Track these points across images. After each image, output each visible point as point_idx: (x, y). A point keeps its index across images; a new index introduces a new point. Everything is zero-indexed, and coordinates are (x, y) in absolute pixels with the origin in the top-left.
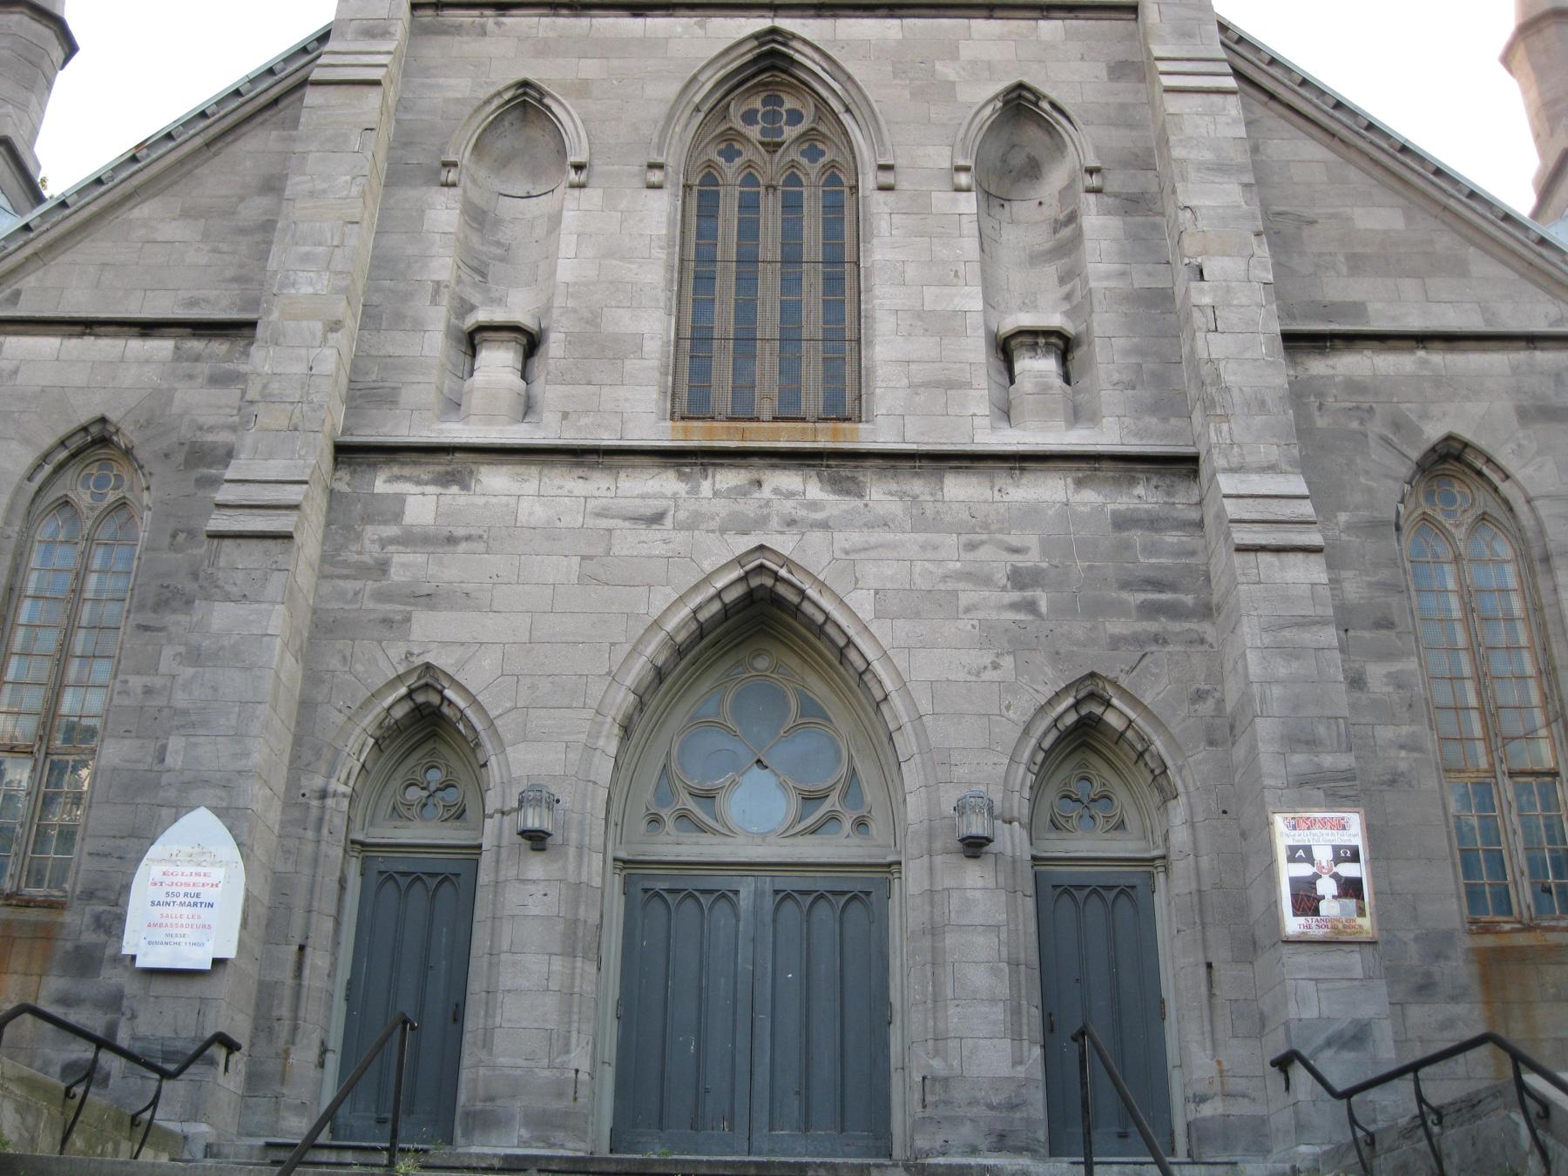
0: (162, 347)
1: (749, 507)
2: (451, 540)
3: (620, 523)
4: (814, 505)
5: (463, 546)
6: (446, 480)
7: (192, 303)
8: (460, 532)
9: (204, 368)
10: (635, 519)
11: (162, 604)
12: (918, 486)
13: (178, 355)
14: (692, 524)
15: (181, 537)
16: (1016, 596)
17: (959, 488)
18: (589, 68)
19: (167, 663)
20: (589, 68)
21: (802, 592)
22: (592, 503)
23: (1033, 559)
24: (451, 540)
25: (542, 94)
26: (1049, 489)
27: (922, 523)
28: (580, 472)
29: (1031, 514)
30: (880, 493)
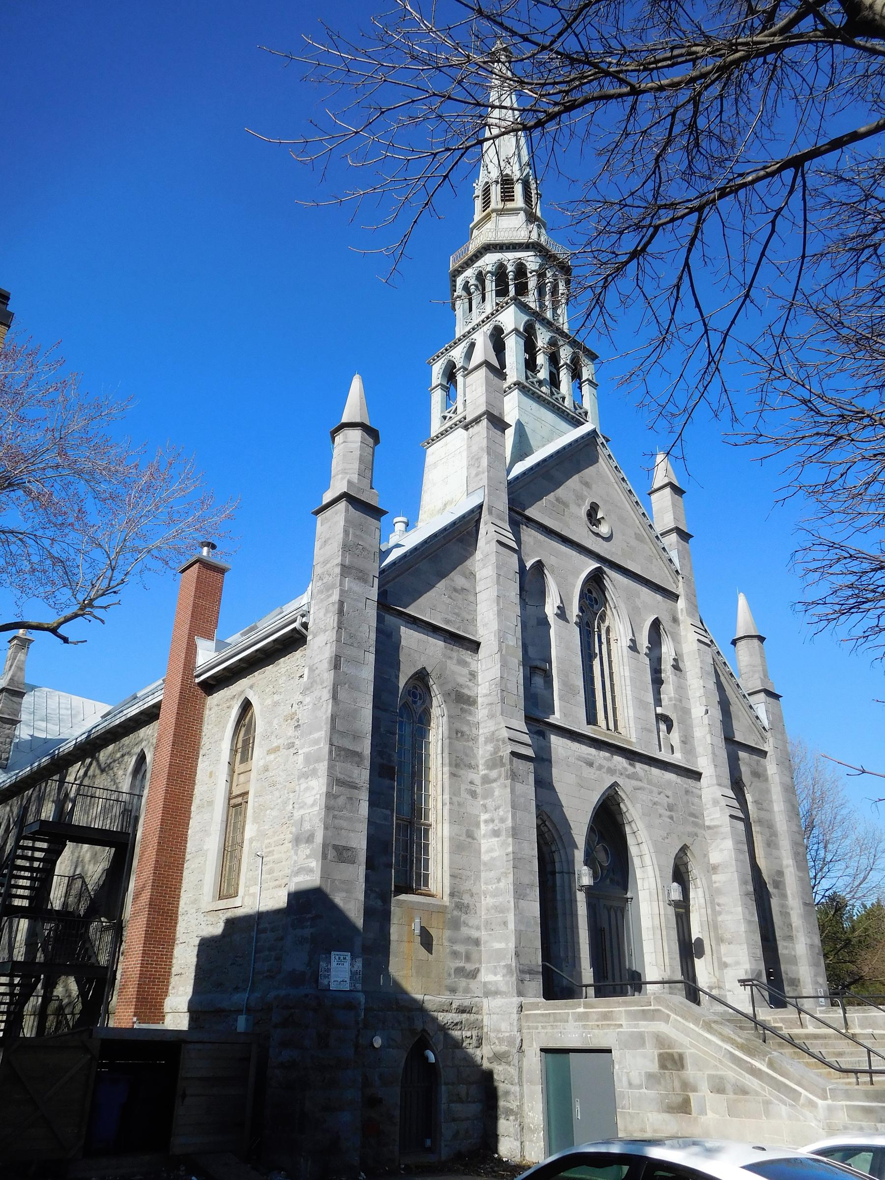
4: (626, 769)
7: (447, 622)
12: (646, 767)
14: (600, 768)
15: (459, 735)
17: (655, 771)
23: (670, 800)
25: (543, 566)
29: (669, 782)
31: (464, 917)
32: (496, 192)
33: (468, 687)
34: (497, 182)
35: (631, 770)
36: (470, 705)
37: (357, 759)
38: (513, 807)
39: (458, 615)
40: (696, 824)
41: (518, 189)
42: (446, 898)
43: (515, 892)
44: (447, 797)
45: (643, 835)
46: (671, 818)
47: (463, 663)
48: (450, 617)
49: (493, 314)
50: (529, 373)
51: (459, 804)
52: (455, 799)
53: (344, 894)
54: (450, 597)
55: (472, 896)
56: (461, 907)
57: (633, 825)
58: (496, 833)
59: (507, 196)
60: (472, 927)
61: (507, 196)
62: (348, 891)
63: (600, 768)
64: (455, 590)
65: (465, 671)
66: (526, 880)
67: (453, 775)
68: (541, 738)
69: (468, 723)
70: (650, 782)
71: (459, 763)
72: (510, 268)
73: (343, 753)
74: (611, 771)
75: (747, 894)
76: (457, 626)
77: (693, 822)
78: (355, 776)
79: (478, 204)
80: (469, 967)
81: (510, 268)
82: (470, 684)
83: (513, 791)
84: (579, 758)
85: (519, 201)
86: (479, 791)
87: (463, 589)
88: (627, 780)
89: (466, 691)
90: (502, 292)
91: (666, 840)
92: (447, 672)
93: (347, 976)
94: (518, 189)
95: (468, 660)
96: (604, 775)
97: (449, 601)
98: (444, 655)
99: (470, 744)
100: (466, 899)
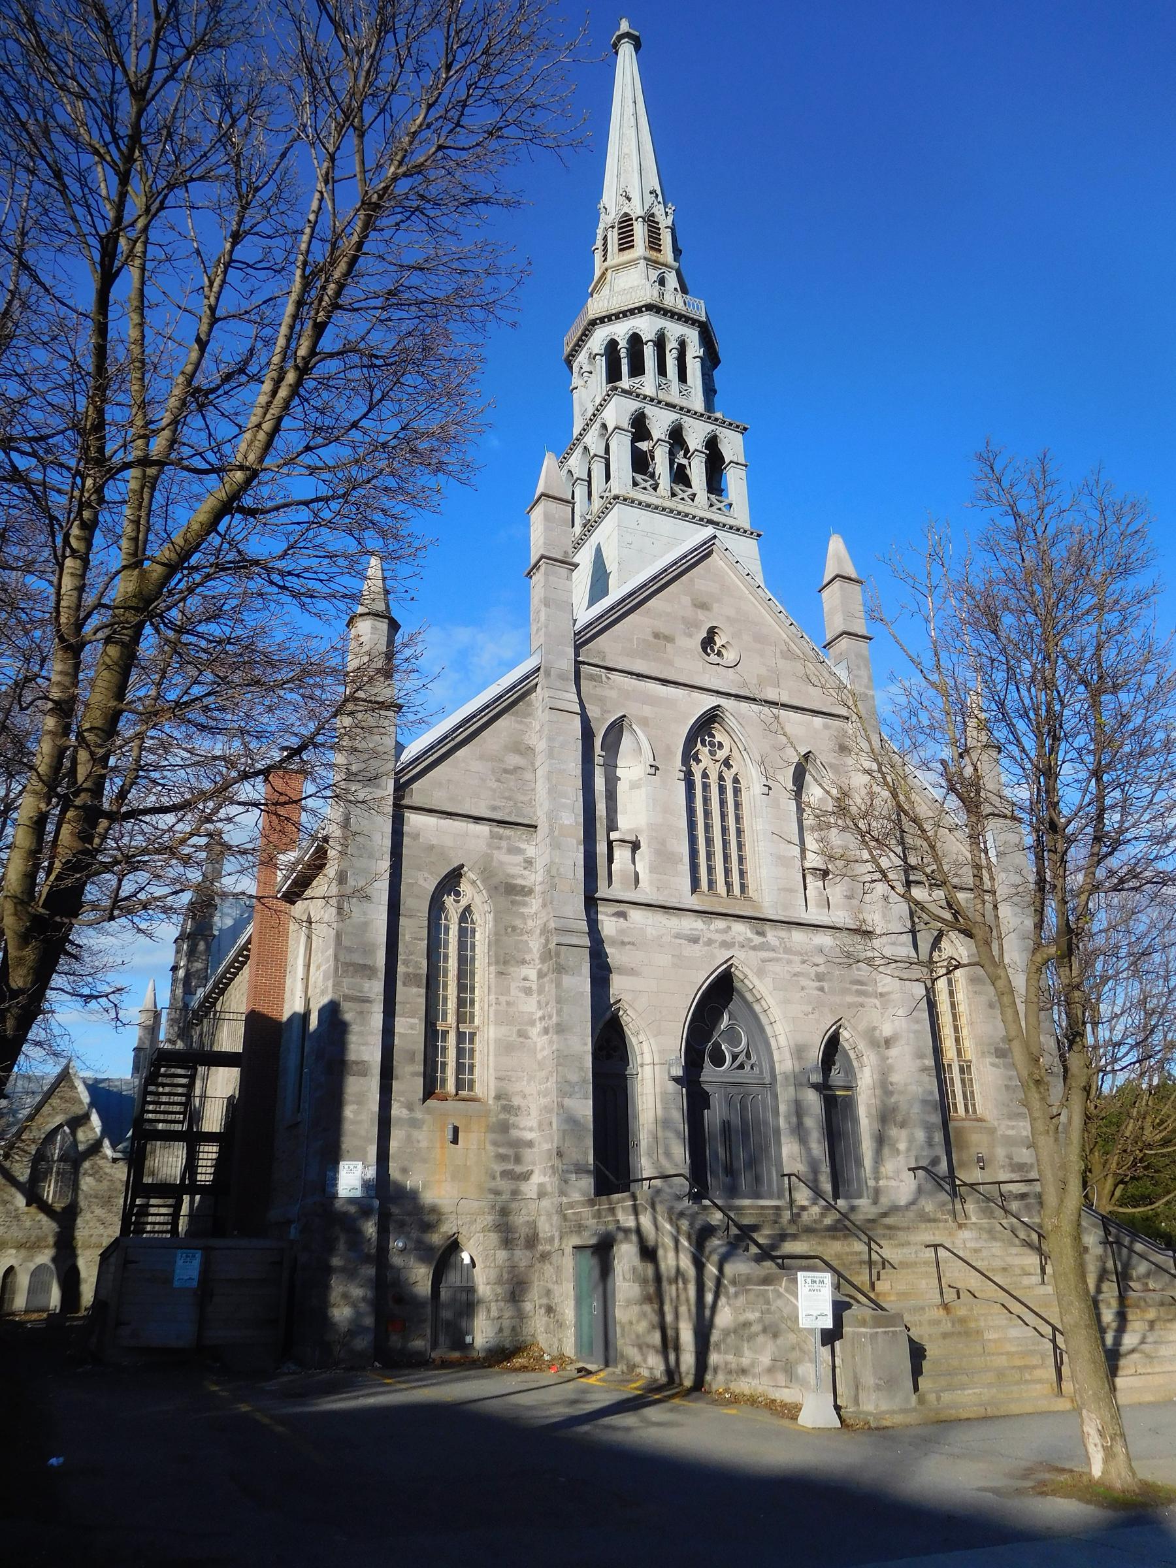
0: (483, 829)
1: (727, 937)
2: (623, 943)
3: (682, 941)
4: (750, 940)
5: (628, 947)
6: (622, 915)
7: (494, 809)
8: (626, 940)
9: (504, 844)
10: (689, 941)
11: (505, 963)
13: (493, 836)
16: (818, 984)
18: (647, 711)
19: (514, 992)
20: (647, 711)
21: (746, 976)
22: (673, 931)
24: (623, 943)
26: (824, 940)
27: (787, 951)
28: (667, 916)
30: (773, 936)
31: (512, 1119)
32: (613, 237)
33: (522, 876)
34: (613, 227)
35: (758, 940)
36: (525, 895)
37: (368, 972)
39: (509, 799)
40: (860, 993)
41: (640, 231)
42: (491, 1102)
44: (492, 997)
45: (776, 1012)
46: (821, 989)
48: (497, 803)
49: (594, 415)
50: (639, 477)
51: (508, 1003)
52: (503, 999)
53: (355, 1107)
54: (498, 781)
55: (524, 1097)
56: (509, 1109)
57: (763, 1002)
58: (546, 1031)
59: (626, 243)
60: (524, 1129)
61: (626, 243)
62: (359, 1103)
63: (710, 942)
64: (506, 771)
65: (519, 859)
66: (574, 1077)
67: (500, 973)
68: (622, 919)
69: (523, 916)
70: (787, 951)
72: (623, 344)
73: (351, 968)
74: (726, 945)
75: (924, 1069)
76: (507, 811)
77: (857, 991)
78: (366, 989)
79: (598, 256)
80: (519, 1169)
81: (623, 344)
82: (526, 873)
83: (558, 985)
84: (678, 936)
86: (534, 987)
87: (517, 769)
88: (752, 953)
89: (519, 882)
90: (613, 374)
91: (810, 1016)
92: (494, 864)
93: (358, 1184)
94: (640, 231)
95: (523, 846)
96: (716, 951)
97: (495, 785)
98: (489, 845)
99: (525, 937)
100: (516, 1101)
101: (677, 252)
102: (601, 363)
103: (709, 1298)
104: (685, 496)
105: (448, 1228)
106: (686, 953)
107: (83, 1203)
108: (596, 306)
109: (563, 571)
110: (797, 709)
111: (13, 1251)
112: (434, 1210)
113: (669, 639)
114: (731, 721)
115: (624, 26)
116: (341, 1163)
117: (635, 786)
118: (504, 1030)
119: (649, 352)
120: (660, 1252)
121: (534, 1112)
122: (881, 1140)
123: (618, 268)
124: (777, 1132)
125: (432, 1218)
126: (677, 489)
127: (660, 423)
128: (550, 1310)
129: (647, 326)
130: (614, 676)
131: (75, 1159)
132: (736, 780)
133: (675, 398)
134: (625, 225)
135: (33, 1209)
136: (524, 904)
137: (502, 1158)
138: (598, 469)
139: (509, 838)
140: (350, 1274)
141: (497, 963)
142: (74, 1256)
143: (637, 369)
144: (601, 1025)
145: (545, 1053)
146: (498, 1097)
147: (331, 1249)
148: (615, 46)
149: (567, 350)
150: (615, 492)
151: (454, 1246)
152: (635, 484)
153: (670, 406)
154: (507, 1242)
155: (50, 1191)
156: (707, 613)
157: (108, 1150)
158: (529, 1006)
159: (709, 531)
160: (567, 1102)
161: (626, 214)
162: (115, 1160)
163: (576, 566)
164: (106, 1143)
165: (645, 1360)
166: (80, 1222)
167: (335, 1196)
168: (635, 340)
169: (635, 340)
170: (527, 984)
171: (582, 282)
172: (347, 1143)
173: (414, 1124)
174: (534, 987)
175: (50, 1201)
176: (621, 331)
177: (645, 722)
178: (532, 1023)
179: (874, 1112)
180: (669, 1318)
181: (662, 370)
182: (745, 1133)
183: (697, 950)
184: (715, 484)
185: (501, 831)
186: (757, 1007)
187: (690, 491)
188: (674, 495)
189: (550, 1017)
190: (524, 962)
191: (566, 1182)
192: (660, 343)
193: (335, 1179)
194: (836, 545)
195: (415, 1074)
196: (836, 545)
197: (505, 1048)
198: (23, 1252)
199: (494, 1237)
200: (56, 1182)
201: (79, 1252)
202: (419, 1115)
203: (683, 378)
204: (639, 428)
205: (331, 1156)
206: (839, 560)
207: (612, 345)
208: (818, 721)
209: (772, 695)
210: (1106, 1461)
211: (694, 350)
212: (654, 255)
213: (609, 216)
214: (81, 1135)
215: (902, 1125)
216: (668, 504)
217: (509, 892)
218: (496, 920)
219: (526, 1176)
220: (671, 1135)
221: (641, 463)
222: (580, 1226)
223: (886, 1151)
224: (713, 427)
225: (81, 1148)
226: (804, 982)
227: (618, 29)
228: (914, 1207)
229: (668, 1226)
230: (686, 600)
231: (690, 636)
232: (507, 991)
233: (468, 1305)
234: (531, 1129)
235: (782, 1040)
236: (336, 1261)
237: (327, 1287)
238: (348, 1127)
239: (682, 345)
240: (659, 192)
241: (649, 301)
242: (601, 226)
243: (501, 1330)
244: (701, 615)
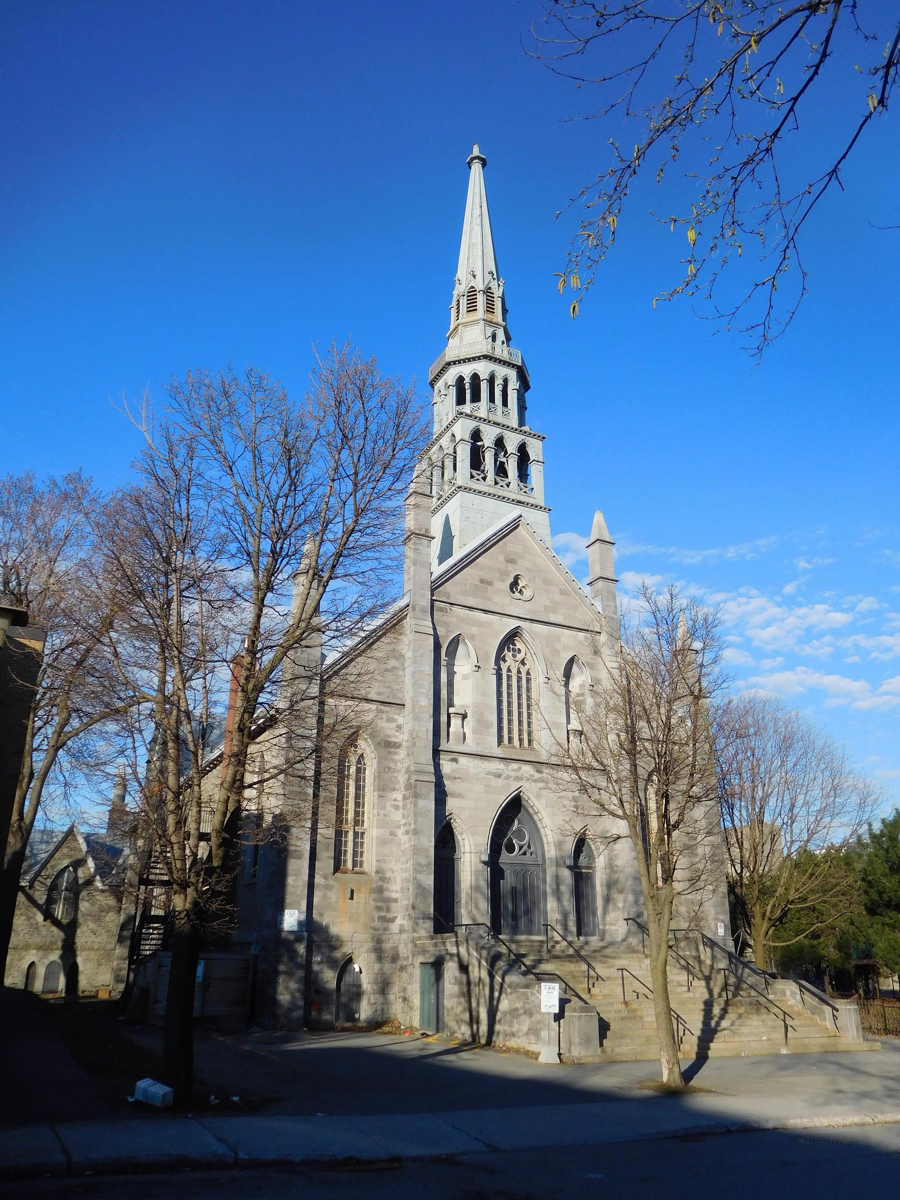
1: (519, 774)
2: (455, 778)
4: (532, 776)
6: (455, 760)
7: (379, 694)
9: (385, 716)
18: (474, 630)
19: (388, 808)
24: (455, 778)
31: (386, 886)
32: (464, 302)
35: (537, 775)
38: (415, 816)
39: (388, 687)
41: (481, 299)
43: (415, 869)
44: (375, 811)
47: (390, 720)
48: (381, 690)
50: (474, 472)
51: (385, 815)
52: (382, 812)
56: (383, 879)
58: (407, 833)
59: (472, 308)
61: (472, 308)
62: (297, 875)
63: (508, 777)
65: (393, 725)
66: (424, 862)
67: (380, 796)
69: (395, 761)
71: (383, 788)
72: (467, 380)
74: (518, 779)
79: (453, 312)
80: (389, 915)
81: (467, 380)
82: (397, 734)
83: (415, 806)
85: (480, 313)
86: (401, 805)
88: (534, 784)
90: (461, 401)
93: (295, 923)
94: (481, 299)
96: (511, 783)
99: (396, 774)
100: (388, 874)
101: (505, 311)
102: (453, 391)
103: (496, 994)
104: (503, 484)
105: (346, 949)
106: (493, 784)
107: (81, 919)
108: (451, 353)
109: (424, 541)
110: (569, 627)
111: (35, 952)
112: (338, 938)
113: (489, 583)
114: (526, 636)
115: (476, 151)
116: (286, 911)
117: (465, 678)
118: (382, 831)
119: (484, 386)
120: (470, 968)
121: (399, 881)
122: (607, 900)
123: (466, 325)
124: (545, 894)
125: (337, 944)
126: (498, 479)
127: (489, 436)
128: (405, 999)
129: (483, 369)
130: (454, 608)
131: (76, 890)
132: (528, 673)
133: (499, 419)
134: (472, 293)
135: (48, 923)
136: (396, 753)
137: (379, 909)
138: (449, 463)
139: (388, 712)
140: (289, 974)
141: (379, 790)
142: (75, 956)
143: (476, 398)
144: (440, 828)
145: (406, 846)
146: (377, 872)
147: (278, 962)
148: (469, 165)
149: (431, 377)
150: (459, 483)
151: (350, 961)
152: (472, 477)
153: (497, 424)
154: (380, 959)
155: (59, 911)
156: (514, 566)
157: (99, 884)
158: (397, 816)
159: (516, 511)
160: (419, 876)
161: (472, 287)
162: (103, 891)
163: (433, 538)
164: (98, 878)
165: (460, 1029)
166: (79, 931)
167: (281, 930)
168: (475, 377)
169: (475, 377)
170: (396, 803)
171: (442, 334)
172: (289, 899)
173: (328, 887)
174: (401, 805)
175: (59, 917)
176: (466, 371)
177: (473, 638)
178: (399, 827)
179: (605, 883)
180: (474, 1005)
181: (492, 399)
182: (525, 895)
183: (499, 782)
184: (523, 475)
185: (383, 708)
186: (535, 817)
187: (507, 481)
188: (496, 483)
189: (410, 825)
190: (394, 789)
191: (417, 924)
192: (491, 380)
193: (282, 920)
194: (598, 518)
195: (329, 858)
196: (598, 518)
197: (382, 842)
198: (41, 952)
199: (373, 956)
200: (64, 905)
201: (78, 953)
202: (331, 882)
203: (505, 403)
204: (476, 435)
205: (280, 907)
206: (600, 528)
207: (461, 379)
208: (581, 635)
209: (553, 618)
210: (669, 1075)
211: (514, 384)
212: (489, 316)
213: (461, 289)
214: (80, 873)
215: (621, 892)
216: (492, 490)
217: (388, 746)
218: (378, 763)
219: (393, 920)
220: (479, 896)
221: (476, 462)
222: (424, 951)
223: (611, 907)
224: (524, 437)
225: (80, 881)
226: (566, 802)
227: (472, 153)
228: (625, 943)
229: (475, 954)
230: (501, 558)
231: (503, 581)
232: (383, 807)
233: (357, 994)
234: (396, 892)
235: (550, 838)
236: (282, 968)
237: (275, 983)
238: (289, 889)
239: (506, 381)
240: (495, 273)
241: (485, 353)
242: (455, 293)
243: (376, 1011)
244: (510, 567)
